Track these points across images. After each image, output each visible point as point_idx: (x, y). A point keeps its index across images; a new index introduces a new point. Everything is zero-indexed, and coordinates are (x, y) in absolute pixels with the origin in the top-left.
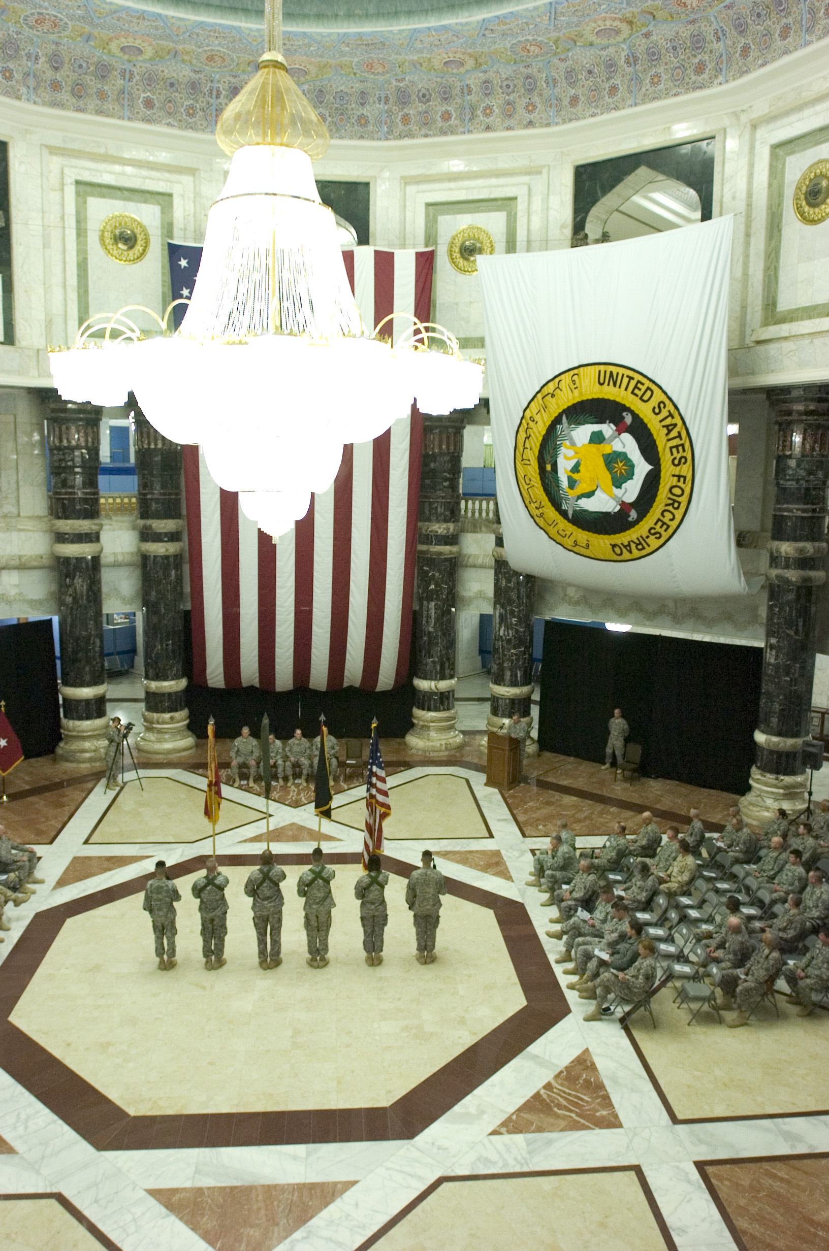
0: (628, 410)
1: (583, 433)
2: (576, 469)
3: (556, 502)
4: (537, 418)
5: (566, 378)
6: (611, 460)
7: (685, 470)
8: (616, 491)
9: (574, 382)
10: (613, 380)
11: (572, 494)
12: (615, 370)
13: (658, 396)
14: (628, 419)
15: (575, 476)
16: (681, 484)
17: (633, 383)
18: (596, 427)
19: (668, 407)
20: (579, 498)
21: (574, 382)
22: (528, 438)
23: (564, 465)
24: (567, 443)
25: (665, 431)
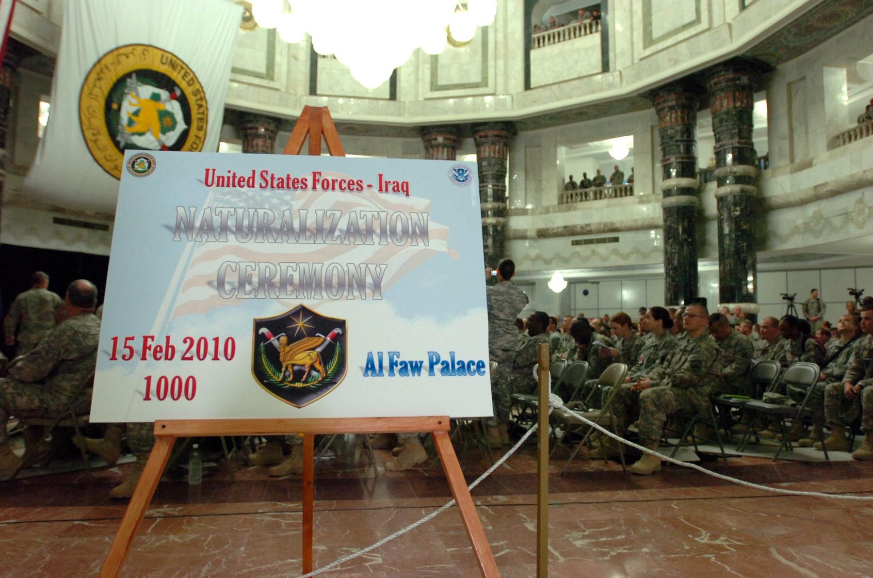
0: (178, 86)
1: (147, 91)
2: (136, 113)
3: (113, 133)
4: (112, 67)
5: (139, 49)
6: (164, 115)
7: (201, 134)
8: (163, 138)
9: (144, 54)
10: (173, 65)
11: (128, 130)
12: (174, 59)
13: (198, 86)
14: (178, 93)
15: (134, 118)
16: (198, 142)
17: (183, 72)
18: (157, 90)
19: (200, 92)
20: (134, 134)
21: (144, 54)
22: (99, 79)
23: (127, 108)
24: (134, 93)
25: (196, 107)
